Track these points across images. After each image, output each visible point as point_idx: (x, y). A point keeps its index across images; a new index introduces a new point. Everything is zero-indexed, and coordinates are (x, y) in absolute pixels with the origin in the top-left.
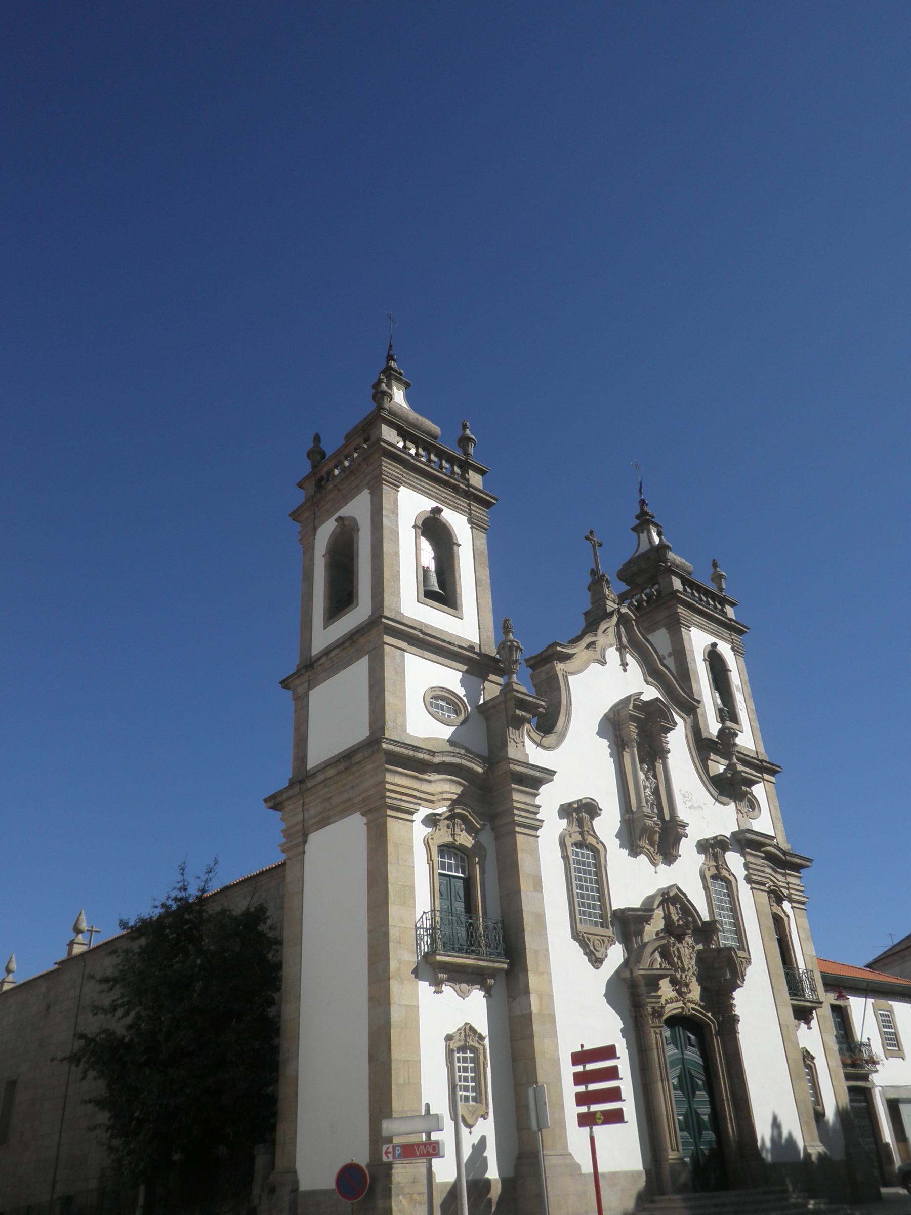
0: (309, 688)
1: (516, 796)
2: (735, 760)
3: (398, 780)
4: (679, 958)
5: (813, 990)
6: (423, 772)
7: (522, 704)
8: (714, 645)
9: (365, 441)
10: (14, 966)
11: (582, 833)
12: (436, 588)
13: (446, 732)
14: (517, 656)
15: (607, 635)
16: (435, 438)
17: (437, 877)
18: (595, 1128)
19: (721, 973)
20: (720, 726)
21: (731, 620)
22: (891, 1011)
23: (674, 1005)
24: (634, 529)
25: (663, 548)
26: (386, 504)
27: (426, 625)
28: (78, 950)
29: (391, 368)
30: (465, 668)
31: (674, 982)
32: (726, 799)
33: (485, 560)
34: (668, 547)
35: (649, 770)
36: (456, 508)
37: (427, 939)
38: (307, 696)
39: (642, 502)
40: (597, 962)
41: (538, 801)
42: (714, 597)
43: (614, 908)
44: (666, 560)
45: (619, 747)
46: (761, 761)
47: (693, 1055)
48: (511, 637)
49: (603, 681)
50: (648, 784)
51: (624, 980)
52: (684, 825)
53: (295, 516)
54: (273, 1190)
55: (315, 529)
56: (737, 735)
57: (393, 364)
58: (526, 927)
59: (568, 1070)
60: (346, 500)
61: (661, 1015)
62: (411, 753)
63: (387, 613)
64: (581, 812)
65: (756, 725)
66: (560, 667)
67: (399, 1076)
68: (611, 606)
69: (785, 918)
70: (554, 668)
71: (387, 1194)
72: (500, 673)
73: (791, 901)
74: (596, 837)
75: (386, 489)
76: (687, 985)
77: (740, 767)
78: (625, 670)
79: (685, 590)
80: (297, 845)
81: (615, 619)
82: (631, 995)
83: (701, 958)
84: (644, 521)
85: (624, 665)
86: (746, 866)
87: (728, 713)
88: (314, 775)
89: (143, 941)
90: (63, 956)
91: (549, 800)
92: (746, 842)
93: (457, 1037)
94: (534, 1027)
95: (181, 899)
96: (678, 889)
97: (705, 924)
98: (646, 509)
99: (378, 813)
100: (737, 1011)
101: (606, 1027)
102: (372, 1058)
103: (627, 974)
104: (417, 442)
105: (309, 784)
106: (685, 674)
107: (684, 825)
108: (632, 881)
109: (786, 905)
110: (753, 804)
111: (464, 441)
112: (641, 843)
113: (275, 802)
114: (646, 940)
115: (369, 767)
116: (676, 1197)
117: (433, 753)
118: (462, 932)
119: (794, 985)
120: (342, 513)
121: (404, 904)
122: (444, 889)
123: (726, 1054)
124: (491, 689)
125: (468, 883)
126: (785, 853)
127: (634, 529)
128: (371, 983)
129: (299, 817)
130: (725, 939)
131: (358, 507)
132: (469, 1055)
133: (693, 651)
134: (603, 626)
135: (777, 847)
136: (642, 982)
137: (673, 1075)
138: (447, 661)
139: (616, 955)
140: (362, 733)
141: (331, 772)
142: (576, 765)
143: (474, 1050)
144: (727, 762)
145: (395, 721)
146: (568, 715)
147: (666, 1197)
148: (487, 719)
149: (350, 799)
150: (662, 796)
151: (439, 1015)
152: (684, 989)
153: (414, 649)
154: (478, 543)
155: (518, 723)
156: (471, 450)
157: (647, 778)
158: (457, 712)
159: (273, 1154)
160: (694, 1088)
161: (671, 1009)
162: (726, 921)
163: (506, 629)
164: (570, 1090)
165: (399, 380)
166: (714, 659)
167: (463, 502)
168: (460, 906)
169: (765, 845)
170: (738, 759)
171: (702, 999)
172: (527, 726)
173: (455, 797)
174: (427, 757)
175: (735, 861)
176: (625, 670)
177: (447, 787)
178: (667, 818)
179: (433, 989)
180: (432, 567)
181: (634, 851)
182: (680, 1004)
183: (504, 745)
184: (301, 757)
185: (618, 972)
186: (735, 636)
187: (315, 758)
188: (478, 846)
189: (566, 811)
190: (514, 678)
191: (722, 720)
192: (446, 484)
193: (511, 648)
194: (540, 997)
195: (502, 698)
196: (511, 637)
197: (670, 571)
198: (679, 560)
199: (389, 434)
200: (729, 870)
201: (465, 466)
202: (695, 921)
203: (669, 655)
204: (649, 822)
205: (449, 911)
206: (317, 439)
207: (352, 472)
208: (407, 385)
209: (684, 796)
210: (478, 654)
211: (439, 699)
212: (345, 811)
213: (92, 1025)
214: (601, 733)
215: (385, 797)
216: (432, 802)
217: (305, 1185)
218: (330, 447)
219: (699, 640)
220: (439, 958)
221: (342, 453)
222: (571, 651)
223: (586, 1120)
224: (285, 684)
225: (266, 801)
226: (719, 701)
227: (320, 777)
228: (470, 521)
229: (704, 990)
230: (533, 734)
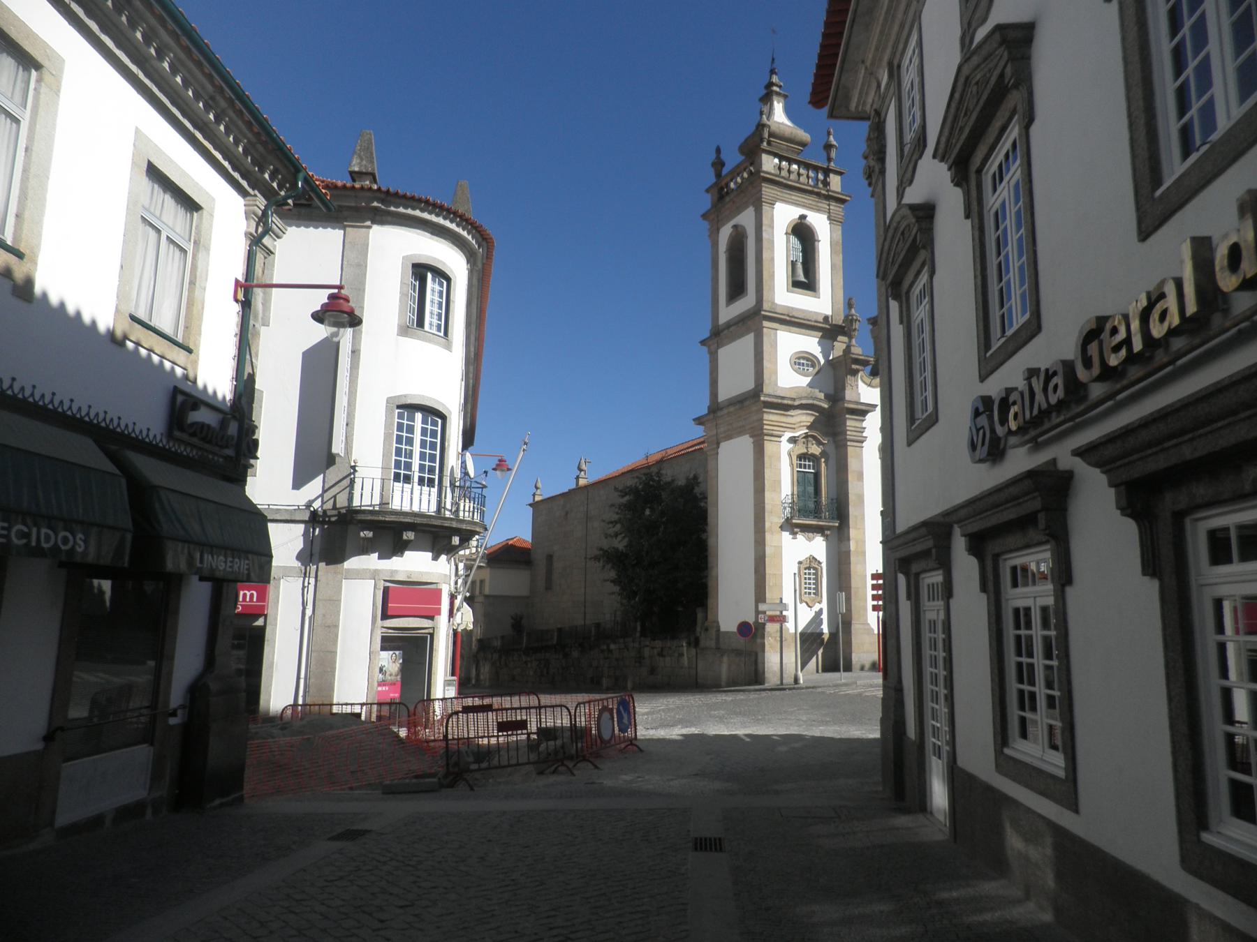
1: (849, 423)
3: (771, 417)
7: (857, 361)
9: (752, 164)
10: (539, 485)
12: (802, 278)
13: (804, 381)
14: (856, 325)
16: (803, 144)
26: (765, 221)
28: (582, 482)
29: (771, 84)
33: (840, 248)
36: (819, 210)
37: (788, 510)
41: (864, 424)
48: (853, 311)
53: (705, 216)
54: (707, 630)
55: (718, 229)
57: (775, 79)
60: (739, 210)
67: (770, 581)
71: (763, 637)
72: (844, 334)
75: (765, 208)
88: (721, 409)
89: (627, 498)
90: (574, 486)
99: (759, 437)
102: (756, 572)
105: (719, 414)
115: (754, 408)
117: (794, 399)
118: (811, 505)
125: (817, 476)
131: (746, 218)
140: (750, 385)
141: (732, 409)
143: (815, 569)
151: (796, 552)
153: (783, 327)
155: (854, 373)
156: (833, 154)
158: (813, 366)
163: (849, 305)
165: (778, 94)
167: (824, 204)
168: (811, 489)
174: (790, 402)
183: (844, 389)
187: (723, 396)
188: (823, 454)
190: (854, 341)
201: (827, 172)
205: (802, 495)
206: (718, 151)
208: (785, 97)
211: (802, 361)
212: (740, 432)
213: (605, 544)
217: (723, 628)
221: (736, 172)
224: (703, 343)
227: (725, 411)
228: (829, 218)
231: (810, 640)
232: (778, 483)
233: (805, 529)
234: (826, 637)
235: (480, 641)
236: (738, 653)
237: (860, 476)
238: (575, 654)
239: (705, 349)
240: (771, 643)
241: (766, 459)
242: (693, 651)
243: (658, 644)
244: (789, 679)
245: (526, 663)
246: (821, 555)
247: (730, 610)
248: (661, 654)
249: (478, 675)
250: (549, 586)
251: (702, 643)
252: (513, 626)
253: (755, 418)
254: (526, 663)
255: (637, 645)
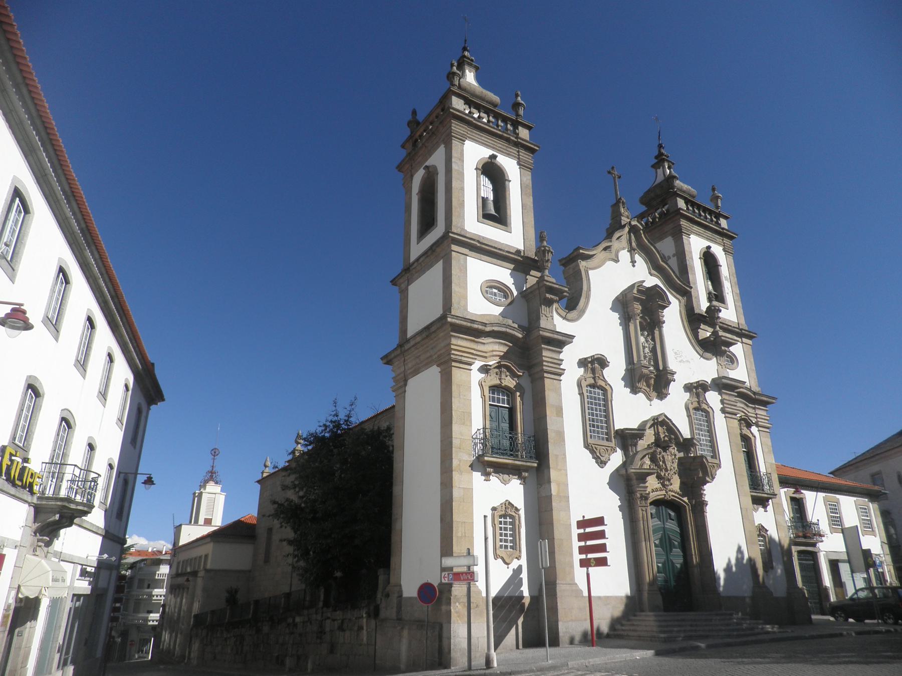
0: (409, 284)
1: (545, 353)
2: (718, 328)
3: (459, 343)
4: (664, 462)
5: (771, 486)
6: (478, 337)
7: (551, 290)
8: (709, 247)
11: (594, 378)
12: (493, 212)
13: (497, 310)
14: (549, 256)
15: (621, 242)
17: (487, 407)
18: (590, 569)
19: (695, 473)
20: (708, 304)
21: (723, 229)
22: (838, 502)
23: (658, 493)
24: (653, 166)
25: (671, 178)
26: (454, 154)
27: (483, 238)
30: (512, 266)
31: (659, 477)
32: (708, 355)
34: (675, 177)
35: (648, 335)
36: (508, 155)
38: (407, 289)
39: (660, 146)
40: (602, 463)
41: (561, 356)
42: (711, 212)
43: (616, 428)
44: (673, 187)
45: (626, 320)
46: (741, 330)
47: (672, 525)
48: (545, 243)
49: (616, 272)
50: (646, 345)
51: (622, 476)
52: (673, 373)
53: (400, 168)
54: (388, 596)
55: (412, 176)
56: (720, 311)
57: (466, 53)
58: (549, 440)
59: (575, 532)
60: (430, 153)
61: (646, 499)
62: (469, 324)
63: (454, 230)
64: (594, 365)
65: (739, 304)
66: (583, 264)
68: (624, 220)
69: (753, 438)
70: (578, 265)
71: (449, 603)
73: (758, 426)
74: (605, 381)
75: (455, 143)
76: (669, 480)
77: (721, 333)
78: (634, 266)
79: (688, 208)
80: (401, 387)
81: (627, 229)
82: (626, 484)
83: (681, 462)
84: (660, 159)
85: (633, 262)
86: (722, 402)
87: (717, 296)
91: (570, 356)
92: (722, 385)
93: (499, 509)
94: (554, 504)
95: (334, 422)
96: (666, 416)
97: (686, 440)
98: (663, 151)
99: (446, 363)
100: (706, 498)
101: (608, 505)
102: (442, 520)
103: (623, 472)
104: (479, 107)
105: (407, 347)
106: (684, 269)
107: (673, 373)
108: (631, 410)
109: (754, 429)
110: (732, 359)
111: (516, 105)
112: (639, 385)
113: (388, 360)
114: (639, 449)
115: (442, 334)
116: (651, 613)
117: (485, 324)
118: (506, 443)
119: (755, 481)
120: (427, 163)
121: (464, 424)
122: (493, 415)
123: (696, 526)
124: (532, 280)
125: (512, 411)
126: (754, 393)
127: (653, 166)
128: (442, 474)
129: (402, 369)
130: (701, 450)
131: (437, 159)
132: (508, 520)
133: (691, 252)
134: (617, 235)
135: (750, 390)
136: (634, 477)
137: (654, 539)
138: (499, 262)
139: (617, 459)
140: (439, 312)
141: (418, 339)
142: (593, 331)
143: (511, 517)
144: (711, 330)
145: (459, 303)
146: (588, 297)
147: (643, 613)
148: (528, 301)
149: (431, 356)
150: (657, 353)
151: (489, 495)
152: (667, 483)
153: (474, 254)
154: (525, 179)
155: (549, 303)
156: (521, 112)
157: (647, 341)
158: (506, 297)
159: (389, 574)
160: (672, 546)
161: (653, 496)
162: (703, 438)
163: (540, 238)
164: (576, 544)
165: (470, 65)
166: (709, 259)
167: (514, 150)
168: (505, 426)
169: (738, 388)
170: (721, 328)
171: (680, 488)
172: (555, 306)
173: (502, 354)
174: (480, 327)
175: (713, 399)
176: (634, 266)
177: (496, 347)
178: (661, 368)
179: (483, 478)
180: (491, 197)
181: (635, 390)
182: (664, 492)
183: (538, 319)
184: (404, 331)
185: (617, 470)
186: (726, 241)
188: (518, 387)
189: (583, 363)
190: (547, 272)
191: (710, 300)
192: (500, 137)
193: (544, 251)
194: (558, 485)
195: (536, 287)
196: (545, 243)
197: (676, 195)
198: (685, 187)
199: (458, 104)
200: (708, 404)
201: (516, 124)
202: (677, 438)
203: (674, 256)
204: (645, 371)
206: (414, 113)
207: (433, 133)
208: (477, 69)
209: (676, 353)
210: (522, 257)
211: (493, 288)
214: (613, 309)
215: (450, 354)
216: (486, 357)
217: (406, 594)
218: (420, 117)
219: (696, 244)
220: (486, 458)
222: (591, 253)
223: (584, 563)
224: (394, 282)
225: (382, 359)
226: (711, 287)
228: (519, 164)
229: (681, 483)
230: (560, 311)
231: (506, 606)
232: (468, 415)
233: (500, 469)
234: (527, 601)
235: (195, 616)
236: (420, 624)
237: (559, 411)
238: (266, 629)
239: (396, 288)
240: (457, 609)
241: (454, 388)
242: (373, 622)
243: (339, 614)
244: (479, 661)
245: (226, 639)
246: (519, 502)
247: (414, 568)
248: (341, 628)
249: (190, 653)
250: (267, 560)
251: (383, 614)
252: (228, 601)
253: (442, 345)
254: (226, 639)
255: (319, 617)
